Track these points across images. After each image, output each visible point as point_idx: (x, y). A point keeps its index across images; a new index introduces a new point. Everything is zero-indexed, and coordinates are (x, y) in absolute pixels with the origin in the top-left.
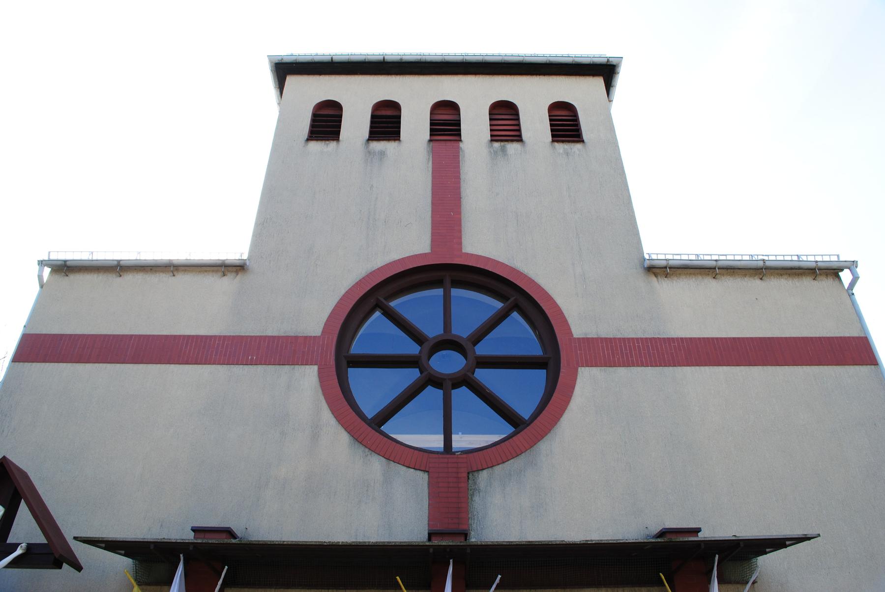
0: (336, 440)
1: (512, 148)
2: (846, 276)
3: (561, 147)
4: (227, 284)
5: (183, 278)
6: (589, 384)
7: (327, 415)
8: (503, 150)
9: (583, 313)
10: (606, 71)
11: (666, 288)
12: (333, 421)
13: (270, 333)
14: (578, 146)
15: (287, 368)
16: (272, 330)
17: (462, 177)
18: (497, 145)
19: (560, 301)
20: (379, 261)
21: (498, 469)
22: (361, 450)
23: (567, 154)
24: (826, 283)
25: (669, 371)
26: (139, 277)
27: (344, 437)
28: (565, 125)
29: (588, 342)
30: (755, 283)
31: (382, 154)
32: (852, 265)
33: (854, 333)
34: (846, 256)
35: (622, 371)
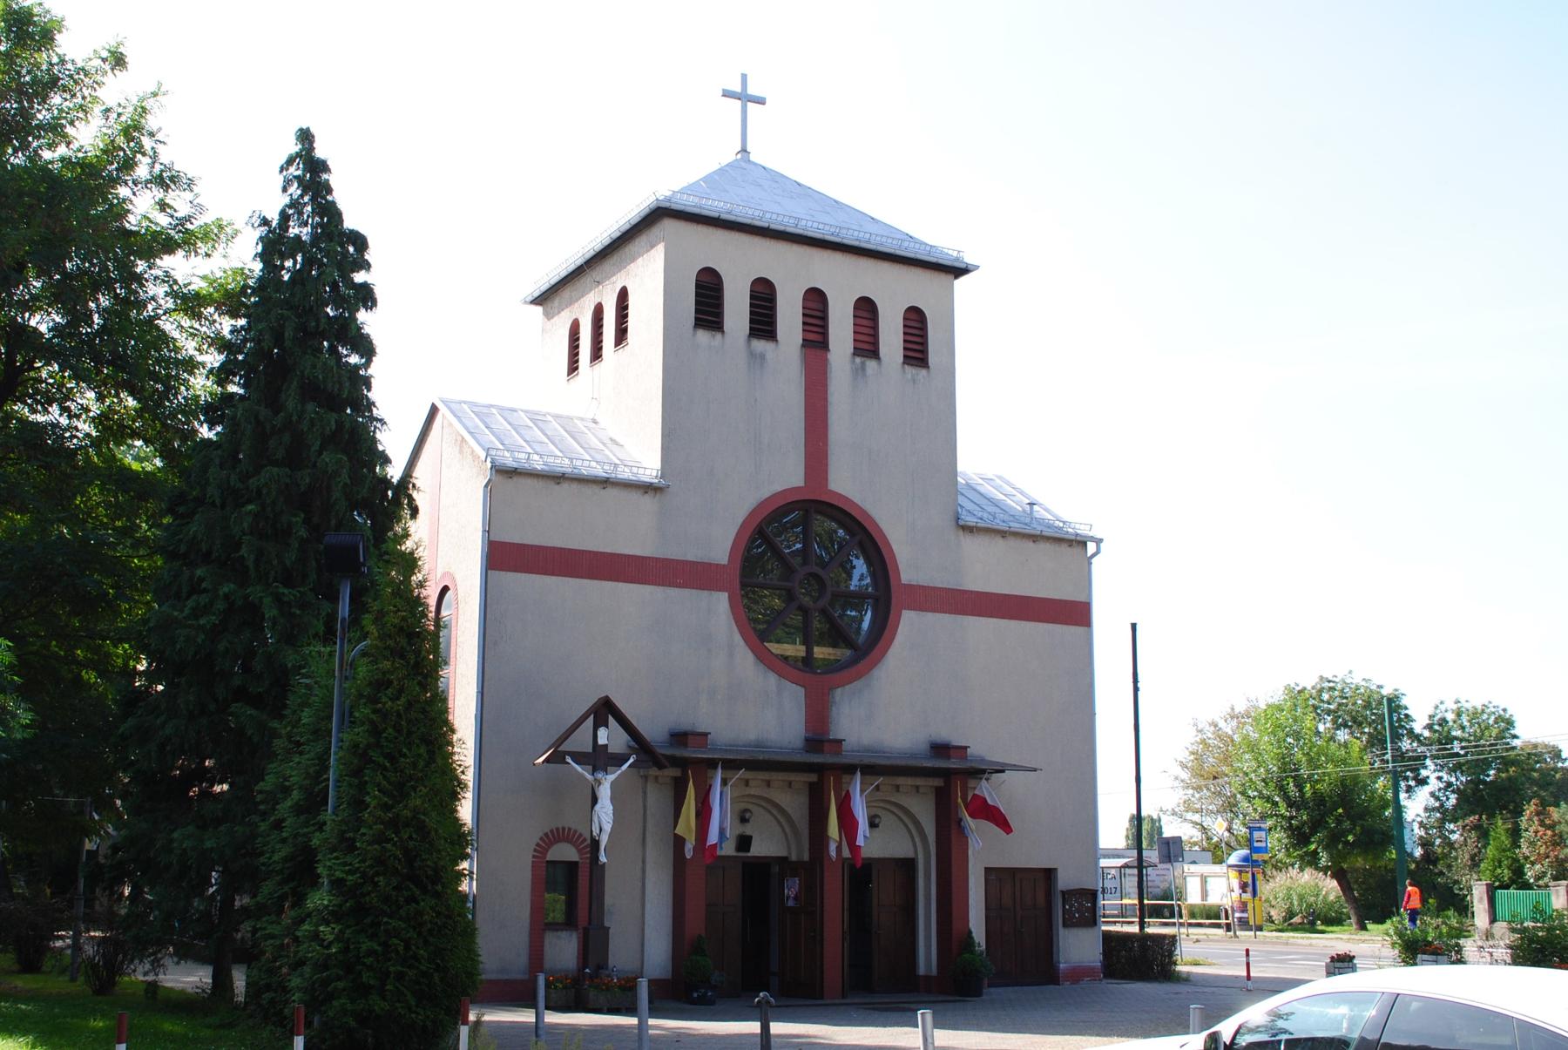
0: (745, 658)
1: (871, 364)
2: (1091, 548)
3: (910, 370)
4: (648, 502)
5: (611, 492)
6: (910, 625)
7: (738, 638)
8: (863, 364)
9: (914, 563)
10: (959, 271)
12: (742, 642)
13: (690, 558)
14: (924, 372)
18: (858, 360)
19: (895, 547)
20: (766, 493)
22: (762, 666)
23: (914, 381)
24: (1077, 550)
25: (960, 618)
26: (575, 486)
27: (750, 657)
29: (911, 588)
31: (762, 357)
32: (1099, 541)
33: (1082, 599)
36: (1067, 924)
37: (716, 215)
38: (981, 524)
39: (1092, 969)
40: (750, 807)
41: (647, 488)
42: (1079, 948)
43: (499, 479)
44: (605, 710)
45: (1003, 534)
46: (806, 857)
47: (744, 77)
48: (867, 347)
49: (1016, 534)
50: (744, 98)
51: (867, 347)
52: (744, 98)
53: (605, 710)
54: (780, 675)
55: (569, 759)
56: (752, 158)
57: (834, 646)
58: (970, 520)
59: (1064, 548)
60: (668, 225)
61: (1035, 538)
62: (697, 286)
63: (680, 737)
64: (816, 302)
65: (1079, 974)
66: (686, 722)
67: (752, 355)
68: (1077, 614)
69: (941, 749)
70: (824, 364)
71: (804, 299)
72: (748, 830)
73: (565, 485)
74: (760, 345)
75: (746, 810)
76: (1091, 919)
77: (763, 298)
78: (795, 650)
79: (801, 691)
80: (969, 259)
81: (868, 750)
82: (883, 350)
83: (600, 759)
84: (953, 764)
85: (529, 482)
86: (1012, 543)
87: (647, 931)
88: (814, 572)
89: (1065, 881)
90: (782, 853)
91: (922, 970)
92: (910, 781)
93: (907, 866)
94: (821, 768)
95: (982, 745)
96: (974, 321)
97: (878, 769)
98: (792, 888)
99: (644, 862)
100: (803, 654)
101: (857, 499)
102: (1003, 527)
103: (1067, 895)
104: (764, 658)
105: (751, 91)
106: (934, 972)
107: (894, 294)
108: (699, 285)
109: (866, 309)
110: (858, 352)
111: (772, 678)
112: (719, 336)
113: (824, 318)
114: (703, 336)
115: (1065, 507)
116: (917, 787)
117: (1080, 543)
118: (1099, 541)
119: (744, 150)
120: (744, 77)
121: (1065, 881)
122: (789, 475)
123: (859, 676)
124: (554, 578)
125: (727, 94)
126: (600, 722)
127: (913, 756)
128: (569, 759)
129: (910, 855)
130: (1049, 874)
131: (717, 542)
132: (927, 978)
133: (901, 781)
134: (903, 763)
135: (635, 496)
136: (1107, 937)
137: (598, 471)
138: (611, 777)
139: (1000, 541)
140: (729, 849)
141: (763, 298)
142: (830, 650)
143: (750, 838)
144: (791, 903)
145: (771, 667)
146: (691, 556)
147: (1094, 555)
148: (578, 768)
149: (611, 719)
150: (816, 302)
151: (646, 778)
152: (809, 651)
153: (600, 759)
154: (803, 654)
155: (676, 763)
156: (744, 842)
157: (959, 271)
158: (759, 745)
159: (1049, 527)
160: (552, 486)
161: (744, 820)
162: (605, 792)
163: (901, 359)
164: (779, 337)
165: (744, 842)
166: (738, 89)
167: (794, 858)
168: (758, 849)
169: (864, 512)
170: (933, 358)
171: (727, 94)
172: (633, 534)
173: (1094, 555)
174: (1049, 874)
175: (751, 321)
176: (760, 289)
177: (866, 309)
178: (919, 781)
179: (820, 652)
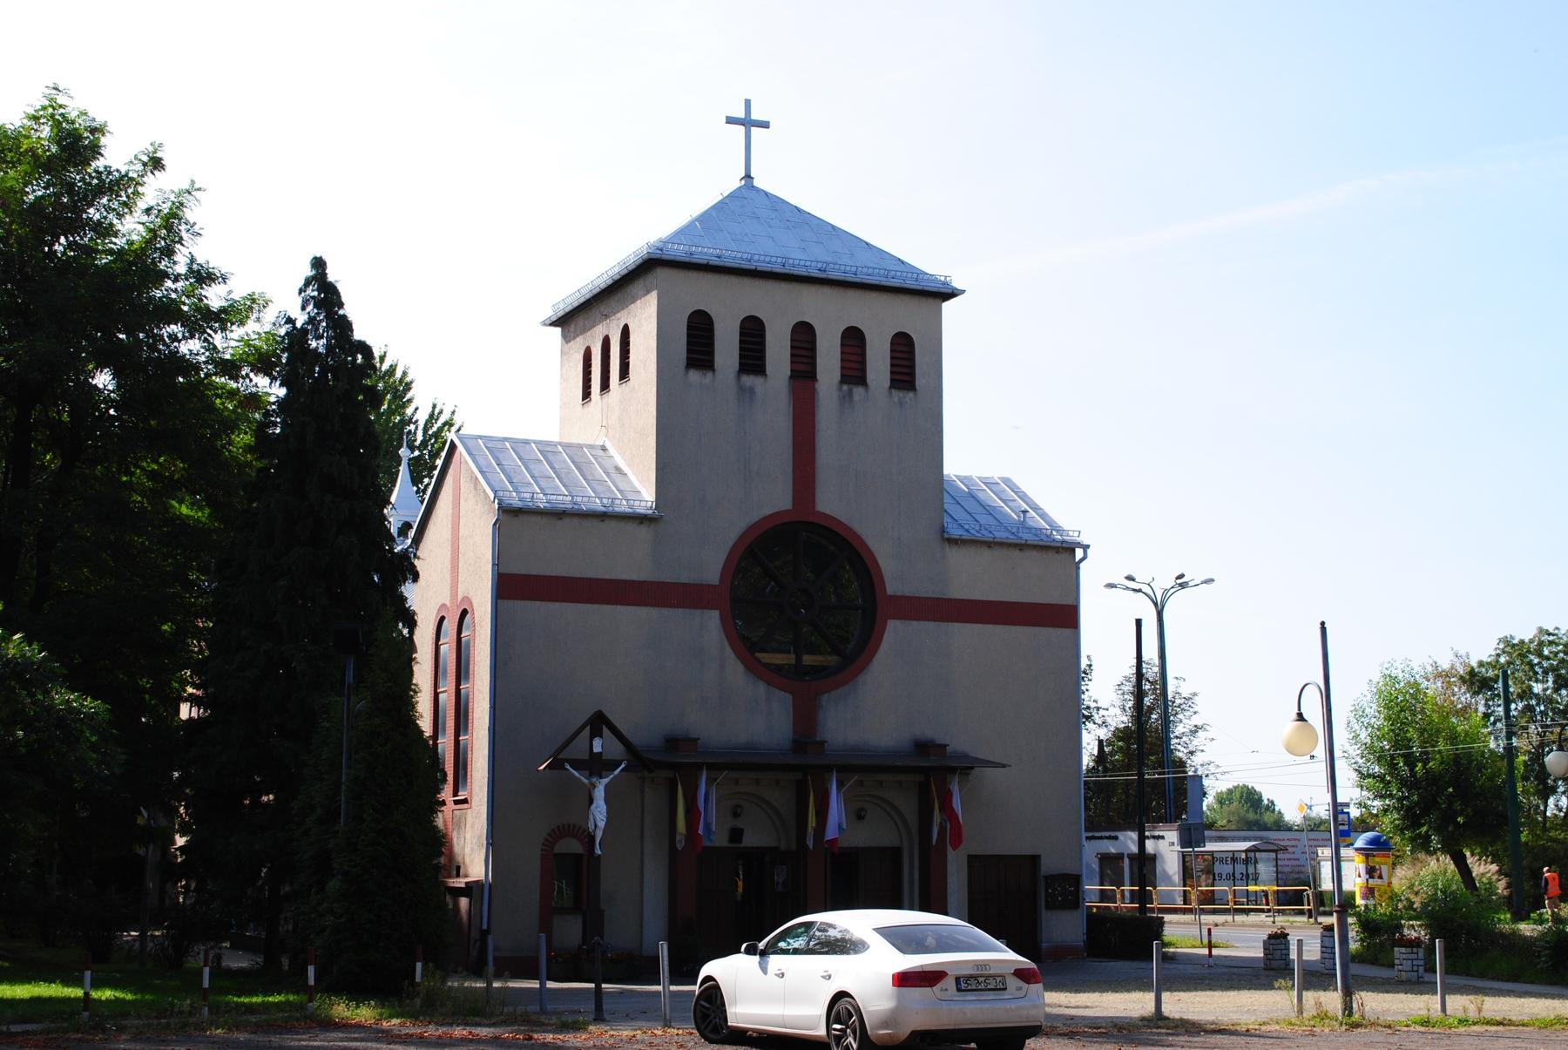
0: (736, 671)
1: (858, 391)
2: (1079, 553)
3: (897, 394)
4: (643, 531)
6: (895, 632)
7: (728, 650)
8: (850, 391)
11: (956, 556)
13: (683, 580)
14: (911, 394)
15: (698, 612)
16: (685, 577)
17: (818, 426)
18: (845, 387)
19: (881, 562)
20: (755, 516)
21: (833, 693)
24: (1065, 556)
25: (944, 625)
26: (575, 521)
27: (740, 668)
28: (903, 347)
30: (1017, 553)
31: (752, 391)
32: (1086, 547)
34: (1084, 540)
35: (915, 623)
36: (1048, 907)
38: (966, 536)
43: (504, 517)
44: (599, 723)
45: (990, 544)
46: (794, 847)
47: (748, 103)
48: (854, 372)
50: (748, 123)
51: (854, 372)
52: (748, 123)
53: (599, 723)
54: (769, 683)
56: (756, 183)
58: (955, 532)
60: (661, 274)
61: (1022, 547)
62: (689, 328)
63: (674, 742)
64: (804, 336)
68: (1066, 616)
69: (924, 747)
70: (812, 393)
72: (739, 824)
73: (567, 520)
74: (748, 380)
77: (752, 331)
79: (789, 697)
80: (957, 284)
83: (597, 765)
89: (1049, 866)
93: (895, 853)
95: (959, 740)
99: (642, 853)
102: (988, 536)
103: (1051, 879)
104: (756, 669)
105: (754, 116)
107: (880, 323)
109: (853, 339)
111: (762, 687)
112: (710, 374)
113: (812, 348)
114: (694, 376)
118: (1086, 547)
119: (748, 176)
120: (748, 103)
121: (1049, 866)
122: (776, 498)
124: (557, 605)
125: (731, 121)
129: (896, 843)
130: (1034, 860)
131: (709, 566)
135: (631, 527)
137: (597, 505)
138: (605, 781)
139: (986, 555)
140: (720, 840)
141: (752, 332)
144: (780, 888)
145: (760, 677)
149: (605, 731)
150: (804, 336)
152: (799, 659)
153: (597, 765)
156: (736, 834)
161: (736, 815)
162: (599, 793)
163: (888, 384)
165: (736, 834)
168: (749, 840)
169: (850, 530)
171: (731, 121)
174: (1034, 860)
175: (741, 356)
177: (853, 339)
179: (808, 659)
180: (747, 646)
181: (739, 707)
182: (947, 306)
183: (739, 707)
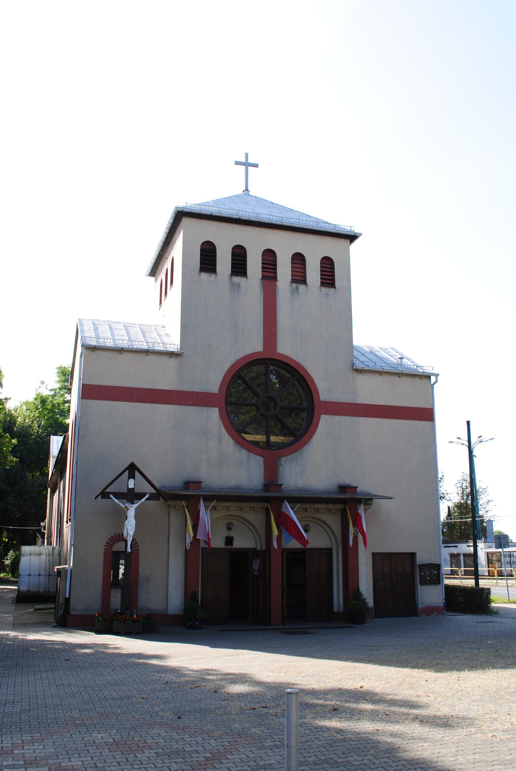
0: (228, 442)
1: (302, 287)
2: (433, 379)
3: (325, 290)
4: (172, 362)
5: (151, 357)
6: (326, 423)
7: (224, 432)
9: (326, 390)
10: (352, 238)
11: (361, 379)
12: (226, 434)
13: (196, 390)
14: (332, 290)
15: (206, 408)
16: (197, 389)
17: (278, 305)
18: (294, 285)
19: (316, 382)
20: (241, 355)
21: (289, 457)
22: (238, 447)
23: (327, 295)
24: (425, 381)
26: (130, 355)
27: (231, 441)
28: (328, 268)
29: (325, 403)
30: (397, 379)
31: (239, 285)
32: (437, 375)
33: (428, 406)
34: (435, 371)
35: (337, 417)
36: (422, 583)
37: (209, 213)
38: (366, 368)
39: (439, 607)
40: (233, 522)
41: (171, 354)
42: (430, 596)
43: (89, 352)
44: (132, 469)
45: (381, 373)
46: (264, 548)
47: (247, 155)
48: (299, 277)
49: (388, 373)
50: (247, 164)
51: (299, 277)
52: (247, 164)
53: (132, 469)
54: (249, 450)
55: (112, 496)
56: (250, 193)
57: (285, 436)
58: (359, 366)
59: (417, 380)
60: (185, 221)
61: (400, 375)
62: (201, 251)
63: (187, 484)
64: (269, 258)
65: (430, 611)
66: (193, 476)
67: (232, 284)
68: (426, 415)
69: (343, 488)
70: (275, 287)
71: (262, 255)
72: (232, 534)
73: (125, 355)
74: (237, 279)
75: (230, 523)
76: (437, 580)
77: (239, 256)
78: (260, 438)
79: (261, 459)
80: (357, 231)
81: (301, 490)
82: (309, 279)
83: (132, 496)
84: (348, 496)
85: (105, 353)
86: (386, 378)
87: (170, 589)
88: (271, 398)
89: (420, 559)
90: (253, 546)
91: (336, 609)
92: (324, 506)
93: (329, 551)
94: (270, 498)
95: (365, 485)
96: (360, 264)
97: (305, 500)
98: (256, 565)
99: (168, 551)
100: (265, 440)
101: (294, 358)
102: (379, 369)
103: (423, 567)
104: (241, 442)
105: (250, 161)
106: (342, 610)
107: (314, 251)
108: (202, 250)
109: (299, 260)
110: (293, 281)
111: (244, 452)
112: (213, 275)
113: (274, 264)
114: (204, 276)
115: (419, 359)
116: (330, 509)
117: (428, 377)
118: (437, 375)
119: (247, 190)
120: (247, 155)
121: (420, 559)
122: (253, 344)
123: (295, 451)
124: (118, 403)
125: (237, 163)
126: (132, 476)
127: (328, 492)
128: (112, 496)
129: (329, 546)
130: (413, 555)
131: (213, 382)
132: (338, 613)
133: (318, 506)
134: (319, 496)
135: (165, 359)
136: (449, 589)
137: (145, 347)
138: (135, 506)
139: (378, 378)
140: (218, 543)
141: (239, 256)
142: (282, 438)
143: (233, 538)
144: (256, 573)
145: (243, 447)
146: (197, 389)
147: (435, 383)
148: (117, 501)
149: (137, 473)
150: (269, 258)
151: (169, 506)
152: (268, 438)
153: (132, 496)
154: (265, 440)
155: (186, 497)
156: (229, 540)
157: (352, 238)
158: (236, 488)
159: (408, 369)
160: (117, 355)
161: (229, 529)
162: (131, 513)
164: (248, 275)
165: (229, 540)
166: (243, 160)
167: (258, 548)
168: (238, 544)
170: (337, 283)
171: (237, 163)
172: (166, 379)
173: (435, 383)
174: (413, 555)
175: (232, 267)
176: (237, 251)
177: (299, 260)
178: (330, 506)
179: (273, 439)
180: (237, 431)
181: (236, 467)
182: (354, 247)
183: (236, 467)
